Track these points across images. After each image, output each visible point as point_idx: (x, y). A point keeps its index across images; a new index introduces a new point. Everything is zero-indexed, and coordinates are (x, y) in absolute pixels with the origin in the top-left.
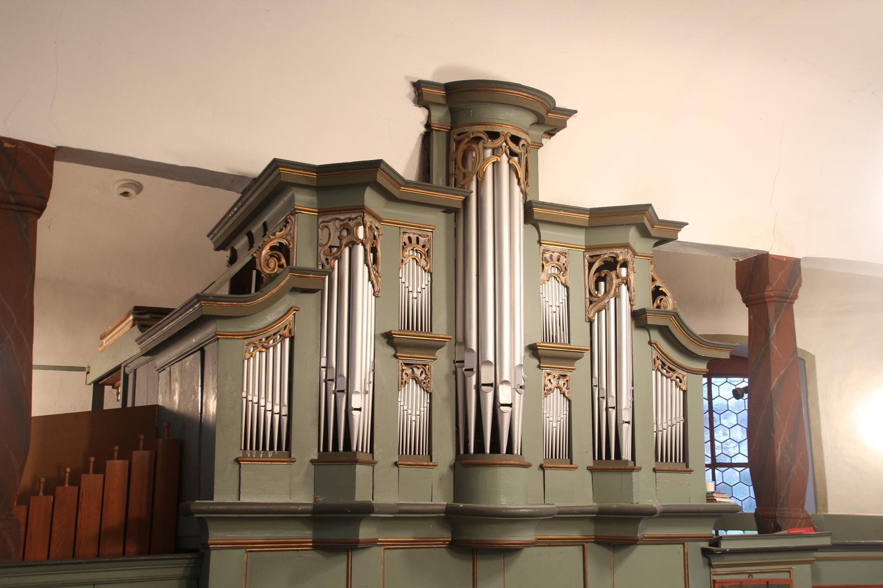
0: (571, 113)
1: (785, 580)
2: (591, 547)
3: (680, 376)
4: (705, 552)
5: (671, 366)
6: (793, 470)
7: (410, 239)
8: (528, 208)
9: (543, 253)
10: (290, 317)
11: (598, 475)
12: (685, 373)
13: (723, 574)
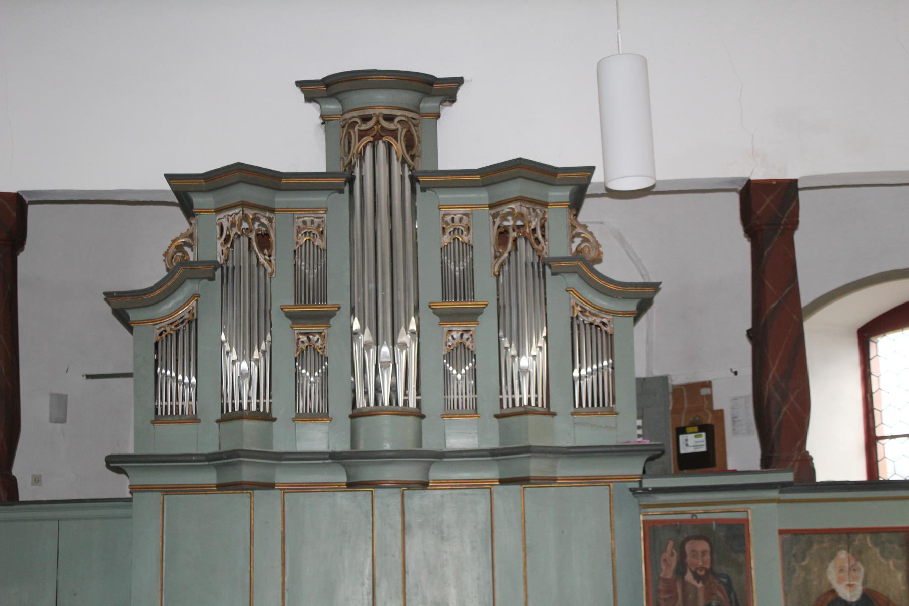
0: (459, 81)
1: (741, 519)
2: (500, 489)
3: (605, 320)
4: (633, 491)
5: (593, 311)
6: (785, 409)
7: (304, 222)
8: (413, 180)
9: (445, 215)
10: (194, 303)
11: (223, 425)
12: (610, 317)
13: (656, 514)
